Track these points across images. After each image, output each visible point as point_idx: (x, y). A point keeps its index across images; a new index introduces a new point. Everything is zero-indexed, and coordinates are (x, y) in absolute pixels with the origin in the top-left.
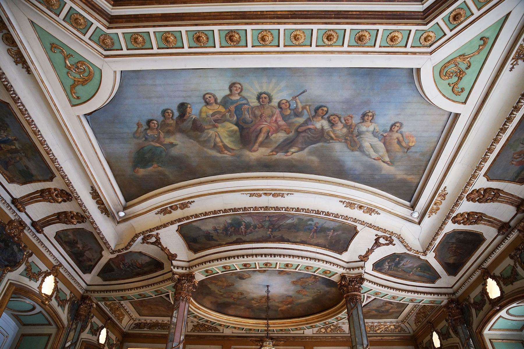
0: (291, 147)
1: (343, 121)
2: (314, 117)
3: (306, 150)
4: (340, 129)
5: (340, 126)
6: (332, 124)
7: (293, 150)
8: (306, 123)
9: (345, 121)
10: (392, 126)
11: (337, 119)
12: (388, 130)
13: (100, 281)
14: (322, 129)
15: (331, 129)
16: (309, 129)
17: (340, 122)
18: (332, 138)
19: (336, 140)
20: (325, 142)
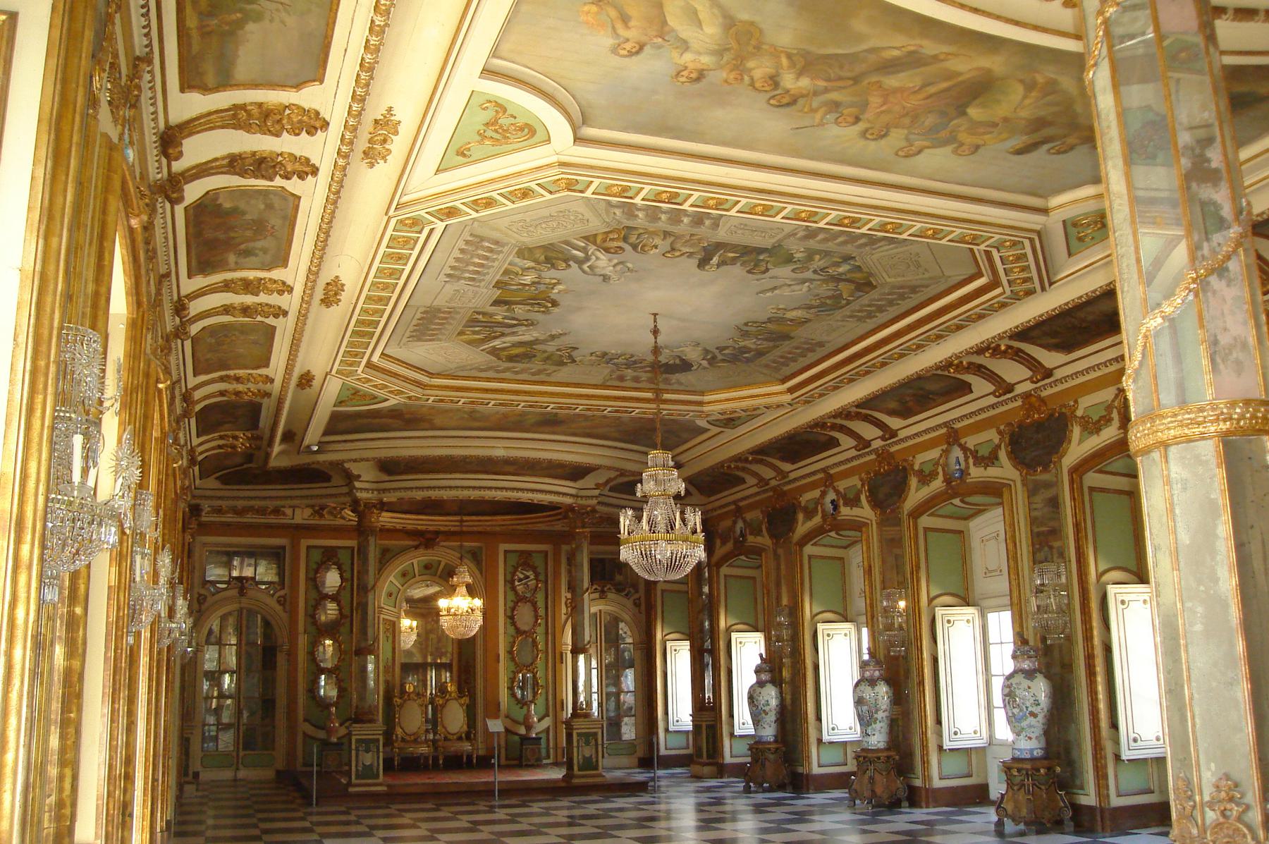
0: (898, 58)
1: (746, 78)
2: (803, 96)
3: (864, 47)
4: (760, 68)
5: (758, 74)
6: (774, 81)
7: (896, 53)
8: (826, 90)
9: (742, 79)
10: (637, 53)
11: (758, 85)
12: (647, 49)
14: (800, 74)
15: (781, 71)
16: (828, 80)
17: (755, 78)
18: (789, 56)
19: (782, 52)
20: (808, 53)
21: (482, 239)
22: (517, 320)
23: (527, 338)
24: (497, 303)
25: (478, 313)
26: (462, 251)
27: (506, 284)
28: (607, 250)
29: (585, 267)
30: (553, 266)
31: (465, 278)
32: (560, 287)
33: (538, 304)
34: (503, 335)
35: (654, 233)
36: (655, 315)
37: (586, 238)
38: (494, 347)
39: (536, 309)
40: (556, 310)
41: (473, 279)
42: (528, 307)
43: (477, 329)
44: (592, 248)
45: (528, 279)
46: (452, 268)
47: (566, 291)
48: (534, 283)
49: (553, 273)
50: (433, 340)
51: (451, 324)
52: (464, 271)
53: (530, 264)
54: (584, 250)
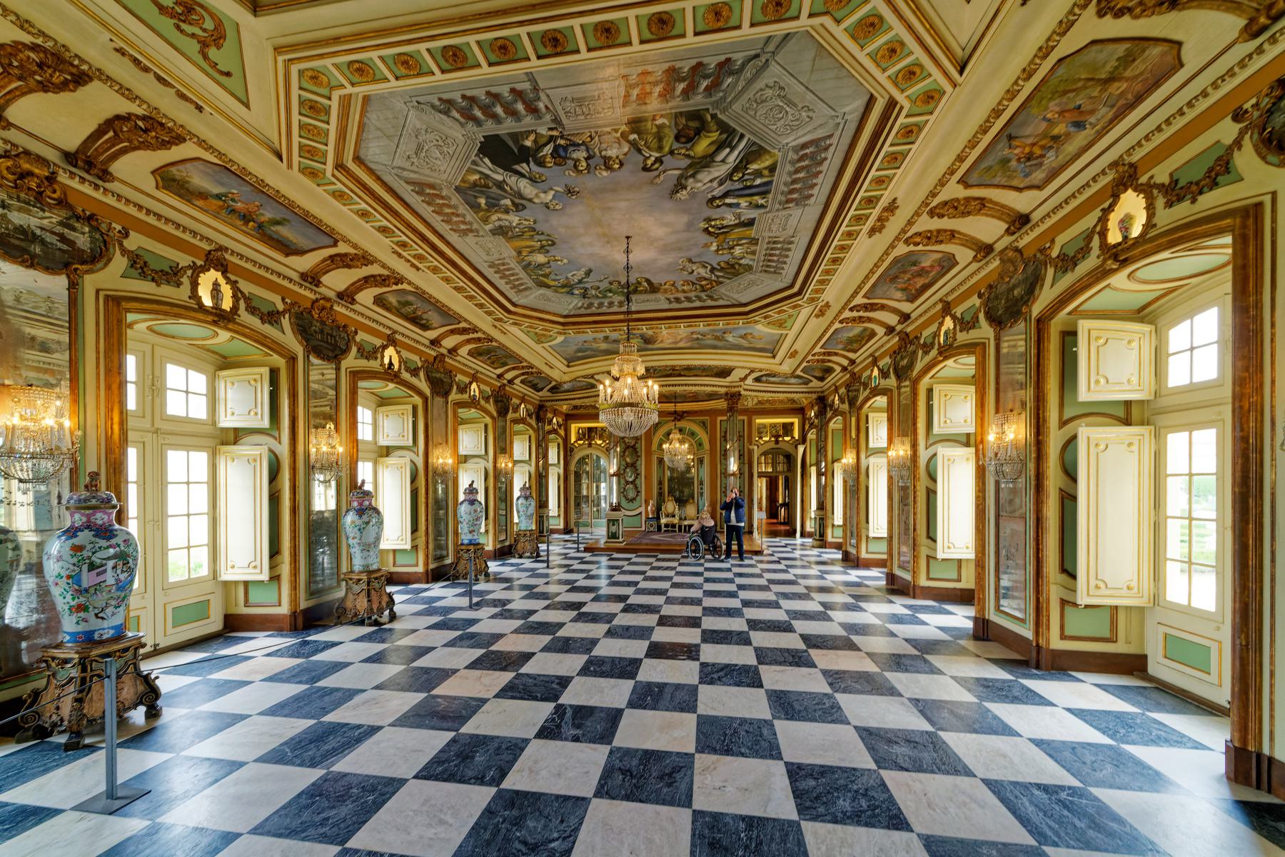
13: (549, 394)
21: (775, 272)
22: (730, 205)
23: (705, 176)
24: (750, 223)
25: (762, 206)
26: (785, 263)
27: (750, 243)
28: (706, 279)
29: (709, 267)
30: (727, 263)
31: (780, 242)
32: (714, 247)
33: (720, 229)
34: (730, 176)
35: (691, 291)
36: (628, 238)
37: (721, 283)
38: (733, 149)
39: (718, 222)
40: (703, 225)
41: (775, 243)
42: (725, 223)
43: (758, 181)
44: (713, 278)
45: (738, 251)
46: (789, 250)
47: (707, 246)
48: (732, 248)
49: (727, 257)
50: (804, 146)
51: (785, 184)
52: (782, 249)
53: (742, 262)
54: (718, 277)
